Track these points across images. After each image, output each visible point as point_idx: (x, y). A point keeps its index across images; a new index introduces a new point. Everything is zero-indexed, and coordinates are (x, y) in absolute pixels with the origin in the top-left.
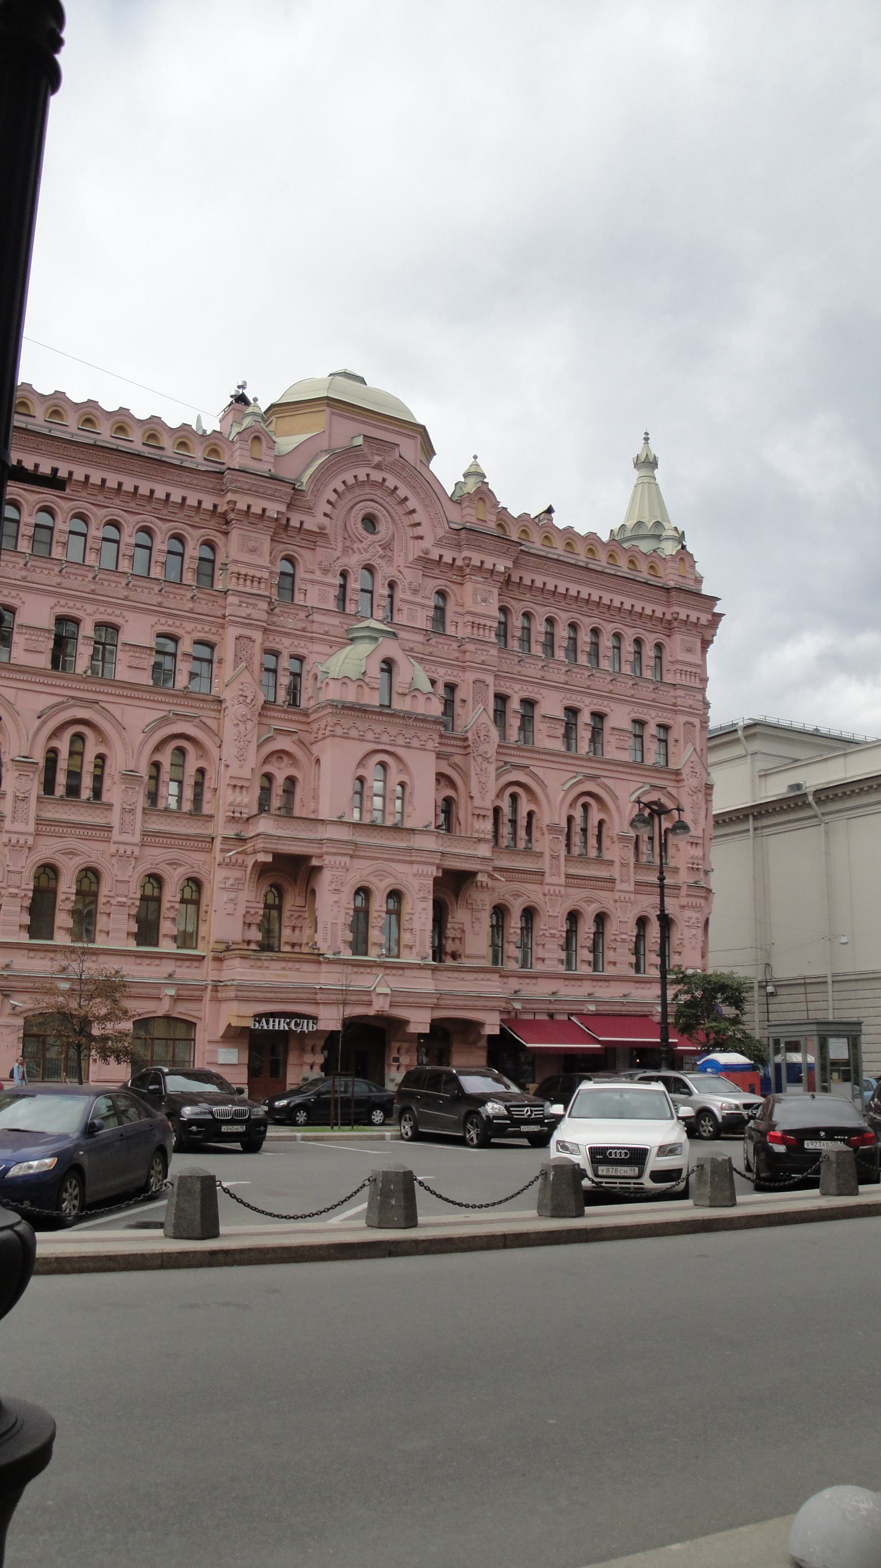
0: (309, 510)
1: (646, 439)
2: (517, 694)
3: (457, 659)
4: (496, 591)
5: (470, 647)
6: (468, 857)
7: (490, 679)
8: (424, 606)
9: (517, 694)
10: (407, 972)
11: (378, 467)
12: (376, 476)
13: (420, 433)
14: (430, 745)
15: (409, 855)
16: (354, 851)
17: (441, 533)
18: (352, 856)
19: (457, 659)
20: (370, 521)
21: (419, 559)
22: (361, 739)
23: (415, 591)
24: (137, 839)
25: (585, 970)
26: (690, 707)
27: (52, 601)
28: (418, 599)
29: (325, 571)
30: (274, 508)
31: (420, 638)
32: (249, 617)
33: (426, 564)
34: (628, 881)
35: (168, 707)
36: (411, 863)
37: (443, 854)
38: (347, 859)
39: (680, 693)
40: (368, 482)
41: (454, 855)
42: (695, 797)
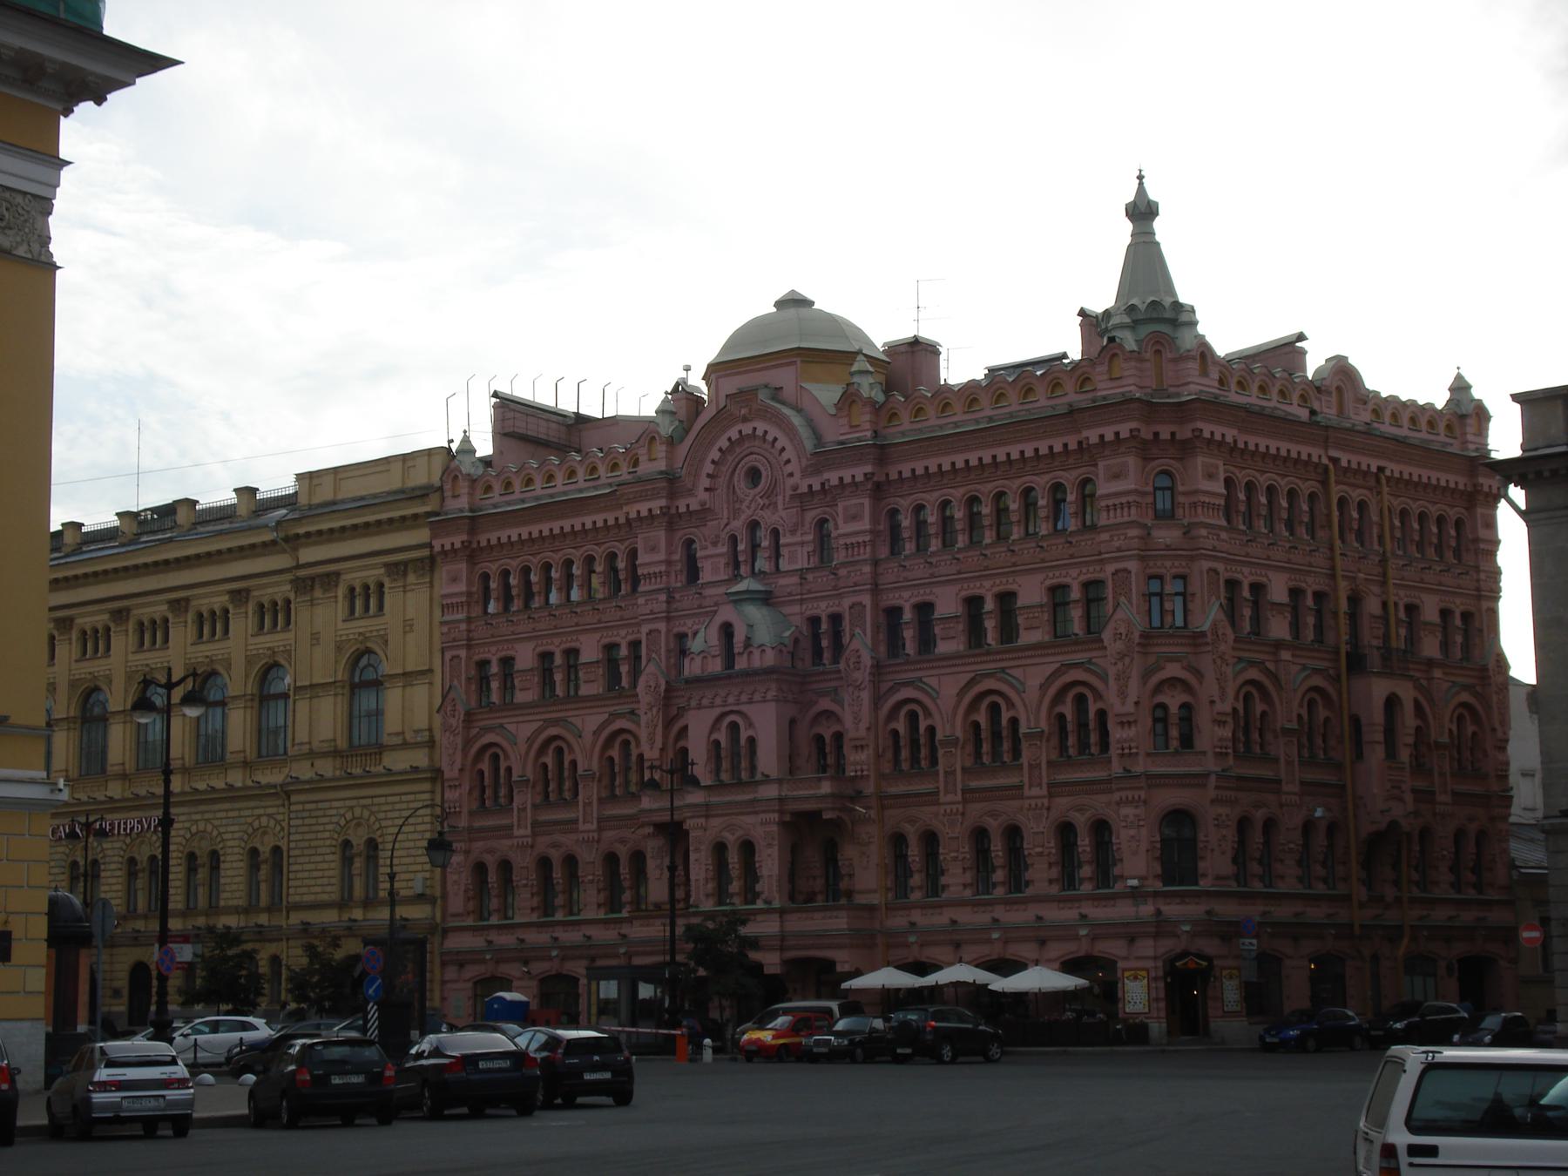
0: (690, 492)
1: (1140, 178)
2: (906, 601)
3: (835, 588)
4: (866, 502)
5: (843, 572)
6: (807, 798)
7: (866, 600)
8: (802, 544)
9: (906, 601)
10: (759, 918)
11: (745, 420)
12: (747, 429)
13: (798, 355)
14: (770, 695)
15: (752, 807)
16: (707, 811)
17: (804, 462)
18: (707, 817)
19: (835, 588)
20: (754, 475)
21: (792, 497)
22: (712, 706)
23: (793, 532)
24: (594, 826)
25: (999, 892)
26: (1119, 550)
27: (532, 645)
28: (797, 539)
29: (715, 544)
30: (657, 505)
31: (795, 579)
32: (652, 613)
33: (803, 499)
34: (1040, 785)
35: (611, 709)
36: (756, 813)
37: (781, 800)
38: (703, 820)
39: (1105, 536)
40: (742, 438)
41: (795, 799)
42: (1120, 666)
